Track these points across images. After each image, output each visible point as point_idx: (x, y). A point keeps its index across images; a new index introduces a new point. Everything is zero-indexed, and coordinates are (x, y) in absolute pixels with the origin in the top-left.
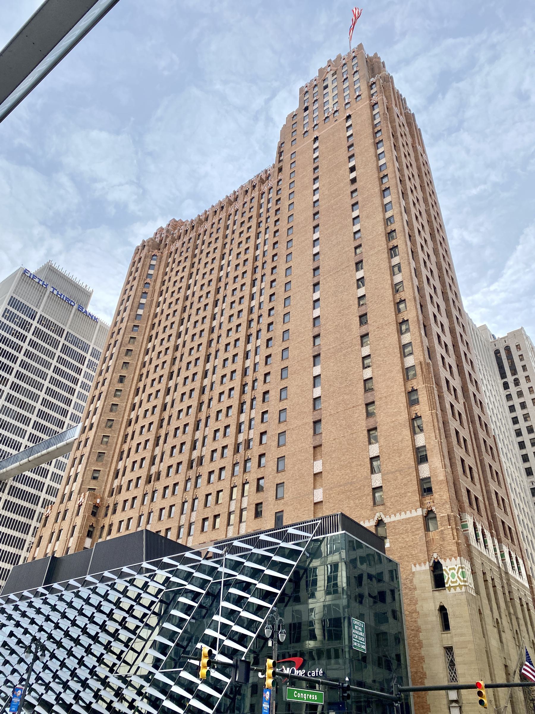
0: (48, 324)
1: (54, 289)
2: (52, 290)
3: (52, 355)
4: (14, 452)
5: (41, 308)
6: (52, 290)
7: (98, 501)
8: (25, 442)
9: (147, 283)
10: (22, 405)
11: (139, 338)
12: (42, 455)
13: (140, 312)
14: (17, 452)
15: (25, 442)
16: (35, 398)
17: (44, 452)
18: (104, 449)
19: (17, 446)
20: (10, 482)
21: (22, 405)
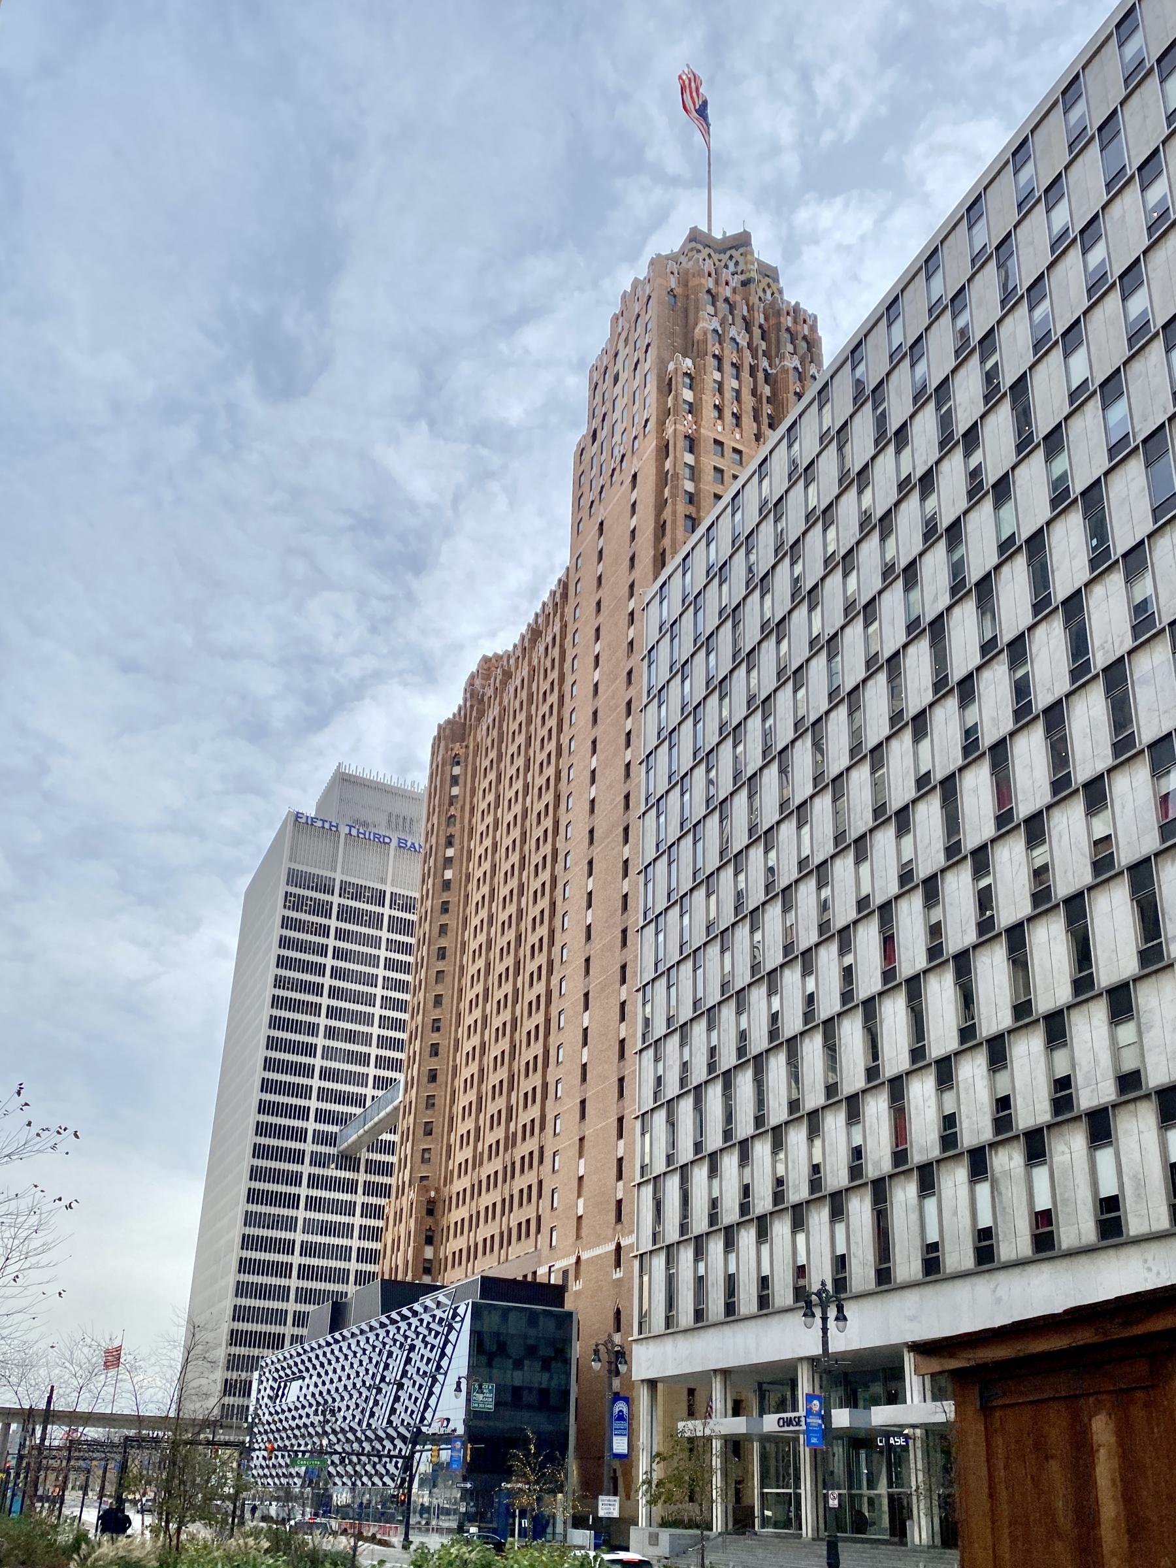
0: (358, 893)
1: (351, 827)
2: (347, 830)
3: (375, 942)
4: (358, 1111)
5: (339, 869)
6: (347, 830)
7: (433, 1194)
8: (369, 1091)
9: (452, 816)
10: (351, 1037)
11: (452, 924)
12: (376, 1124)
13: (448, 874)
14: (362, 1110)
15: (369, 1091)
16: (367, 1019)
17: (376, 1119)
18: (431, 1117)
19: (359, 1101)
20: (364, 1155)
21: (351, 1037)
